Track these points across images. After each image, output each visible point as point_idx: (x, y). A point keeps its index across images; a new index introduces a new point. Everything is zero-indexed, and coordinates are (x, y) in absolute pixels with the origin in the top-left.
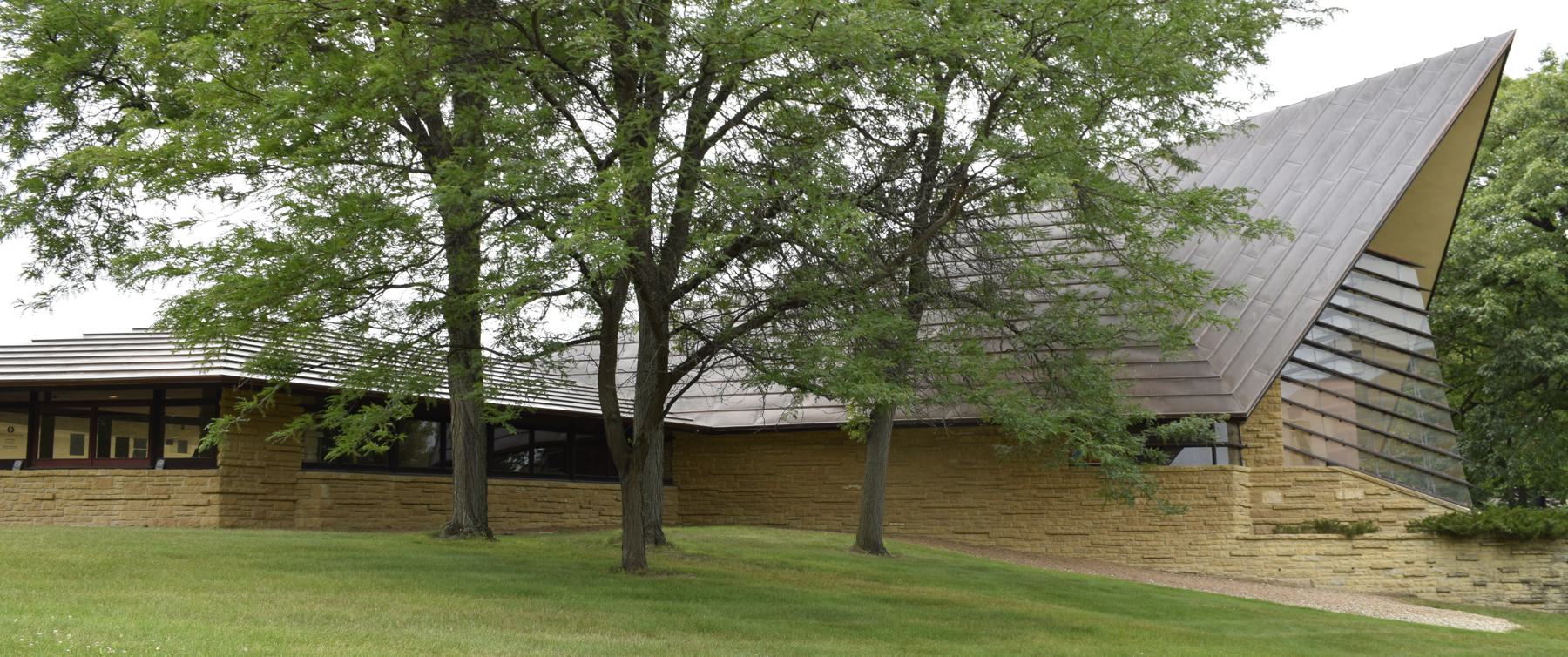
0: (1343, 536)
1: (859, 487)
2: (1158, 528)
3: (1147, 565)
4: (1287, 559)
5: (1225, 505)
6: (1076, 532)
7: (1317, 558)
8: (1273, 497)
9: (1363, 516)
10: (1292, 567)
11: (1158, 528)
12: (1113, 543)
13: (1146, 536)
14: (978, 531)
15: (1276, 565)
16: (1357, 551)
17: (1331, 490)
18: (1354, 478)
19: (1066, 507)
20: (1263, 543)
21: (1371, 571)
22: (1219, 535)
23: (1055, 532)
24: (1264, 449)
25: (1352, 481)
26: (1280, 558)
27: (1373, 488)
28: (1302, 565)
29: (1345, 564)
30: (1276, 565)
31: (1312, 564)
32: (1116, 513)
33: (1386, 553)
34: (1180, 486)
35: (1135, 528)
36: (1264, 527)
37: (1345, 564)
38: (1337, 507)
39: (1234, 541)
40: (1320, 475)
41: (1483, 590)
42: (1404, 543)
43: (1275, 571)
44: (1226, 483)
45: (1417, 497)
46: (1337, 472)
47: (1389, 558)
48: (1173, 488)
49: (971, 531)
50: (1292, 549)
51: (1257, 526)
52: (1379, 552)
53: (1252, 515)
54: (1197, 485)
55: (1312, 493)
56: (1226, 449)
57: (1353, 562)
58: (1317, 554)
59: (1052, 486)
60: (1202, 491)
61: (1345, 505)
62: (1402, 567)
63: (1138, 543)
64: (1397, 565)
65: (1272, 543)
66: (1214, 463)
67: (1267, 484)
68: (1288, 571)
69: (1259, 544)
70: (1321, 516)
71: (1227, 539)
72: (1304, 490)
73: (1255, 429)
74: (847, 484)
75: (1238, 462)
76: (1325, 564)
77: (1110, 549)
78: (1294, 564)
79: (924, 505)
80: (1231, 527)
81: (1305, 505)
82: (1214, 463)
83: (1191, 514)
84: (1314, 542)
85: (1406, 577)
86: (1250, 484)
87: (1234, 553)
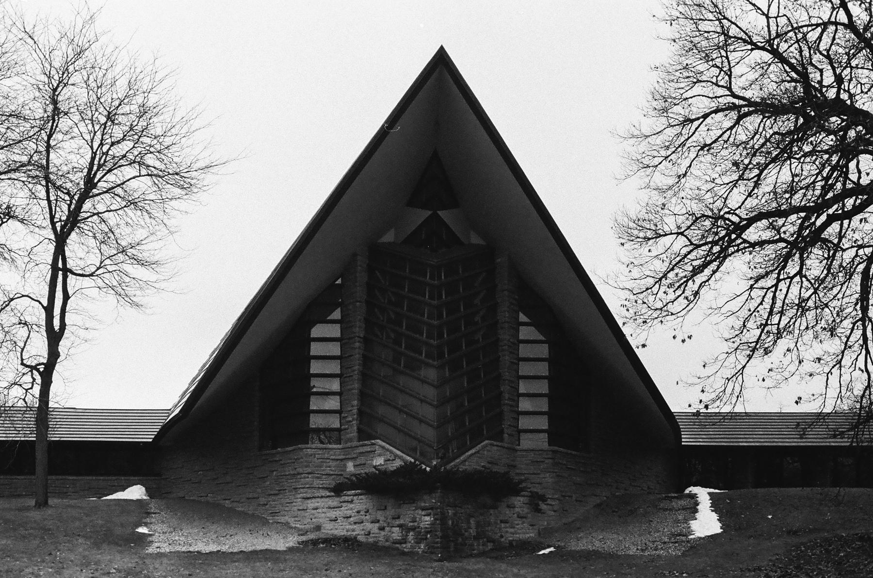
4: (315, 511)
11: (277, 492)
27: (388, 456)
29: (333, 514)
37: (333, 514)
46: (373, 444)
62: (355, 516)
69: (309, 501)
80: (302, 490)
83: (289, 481)
85: (355, 523)
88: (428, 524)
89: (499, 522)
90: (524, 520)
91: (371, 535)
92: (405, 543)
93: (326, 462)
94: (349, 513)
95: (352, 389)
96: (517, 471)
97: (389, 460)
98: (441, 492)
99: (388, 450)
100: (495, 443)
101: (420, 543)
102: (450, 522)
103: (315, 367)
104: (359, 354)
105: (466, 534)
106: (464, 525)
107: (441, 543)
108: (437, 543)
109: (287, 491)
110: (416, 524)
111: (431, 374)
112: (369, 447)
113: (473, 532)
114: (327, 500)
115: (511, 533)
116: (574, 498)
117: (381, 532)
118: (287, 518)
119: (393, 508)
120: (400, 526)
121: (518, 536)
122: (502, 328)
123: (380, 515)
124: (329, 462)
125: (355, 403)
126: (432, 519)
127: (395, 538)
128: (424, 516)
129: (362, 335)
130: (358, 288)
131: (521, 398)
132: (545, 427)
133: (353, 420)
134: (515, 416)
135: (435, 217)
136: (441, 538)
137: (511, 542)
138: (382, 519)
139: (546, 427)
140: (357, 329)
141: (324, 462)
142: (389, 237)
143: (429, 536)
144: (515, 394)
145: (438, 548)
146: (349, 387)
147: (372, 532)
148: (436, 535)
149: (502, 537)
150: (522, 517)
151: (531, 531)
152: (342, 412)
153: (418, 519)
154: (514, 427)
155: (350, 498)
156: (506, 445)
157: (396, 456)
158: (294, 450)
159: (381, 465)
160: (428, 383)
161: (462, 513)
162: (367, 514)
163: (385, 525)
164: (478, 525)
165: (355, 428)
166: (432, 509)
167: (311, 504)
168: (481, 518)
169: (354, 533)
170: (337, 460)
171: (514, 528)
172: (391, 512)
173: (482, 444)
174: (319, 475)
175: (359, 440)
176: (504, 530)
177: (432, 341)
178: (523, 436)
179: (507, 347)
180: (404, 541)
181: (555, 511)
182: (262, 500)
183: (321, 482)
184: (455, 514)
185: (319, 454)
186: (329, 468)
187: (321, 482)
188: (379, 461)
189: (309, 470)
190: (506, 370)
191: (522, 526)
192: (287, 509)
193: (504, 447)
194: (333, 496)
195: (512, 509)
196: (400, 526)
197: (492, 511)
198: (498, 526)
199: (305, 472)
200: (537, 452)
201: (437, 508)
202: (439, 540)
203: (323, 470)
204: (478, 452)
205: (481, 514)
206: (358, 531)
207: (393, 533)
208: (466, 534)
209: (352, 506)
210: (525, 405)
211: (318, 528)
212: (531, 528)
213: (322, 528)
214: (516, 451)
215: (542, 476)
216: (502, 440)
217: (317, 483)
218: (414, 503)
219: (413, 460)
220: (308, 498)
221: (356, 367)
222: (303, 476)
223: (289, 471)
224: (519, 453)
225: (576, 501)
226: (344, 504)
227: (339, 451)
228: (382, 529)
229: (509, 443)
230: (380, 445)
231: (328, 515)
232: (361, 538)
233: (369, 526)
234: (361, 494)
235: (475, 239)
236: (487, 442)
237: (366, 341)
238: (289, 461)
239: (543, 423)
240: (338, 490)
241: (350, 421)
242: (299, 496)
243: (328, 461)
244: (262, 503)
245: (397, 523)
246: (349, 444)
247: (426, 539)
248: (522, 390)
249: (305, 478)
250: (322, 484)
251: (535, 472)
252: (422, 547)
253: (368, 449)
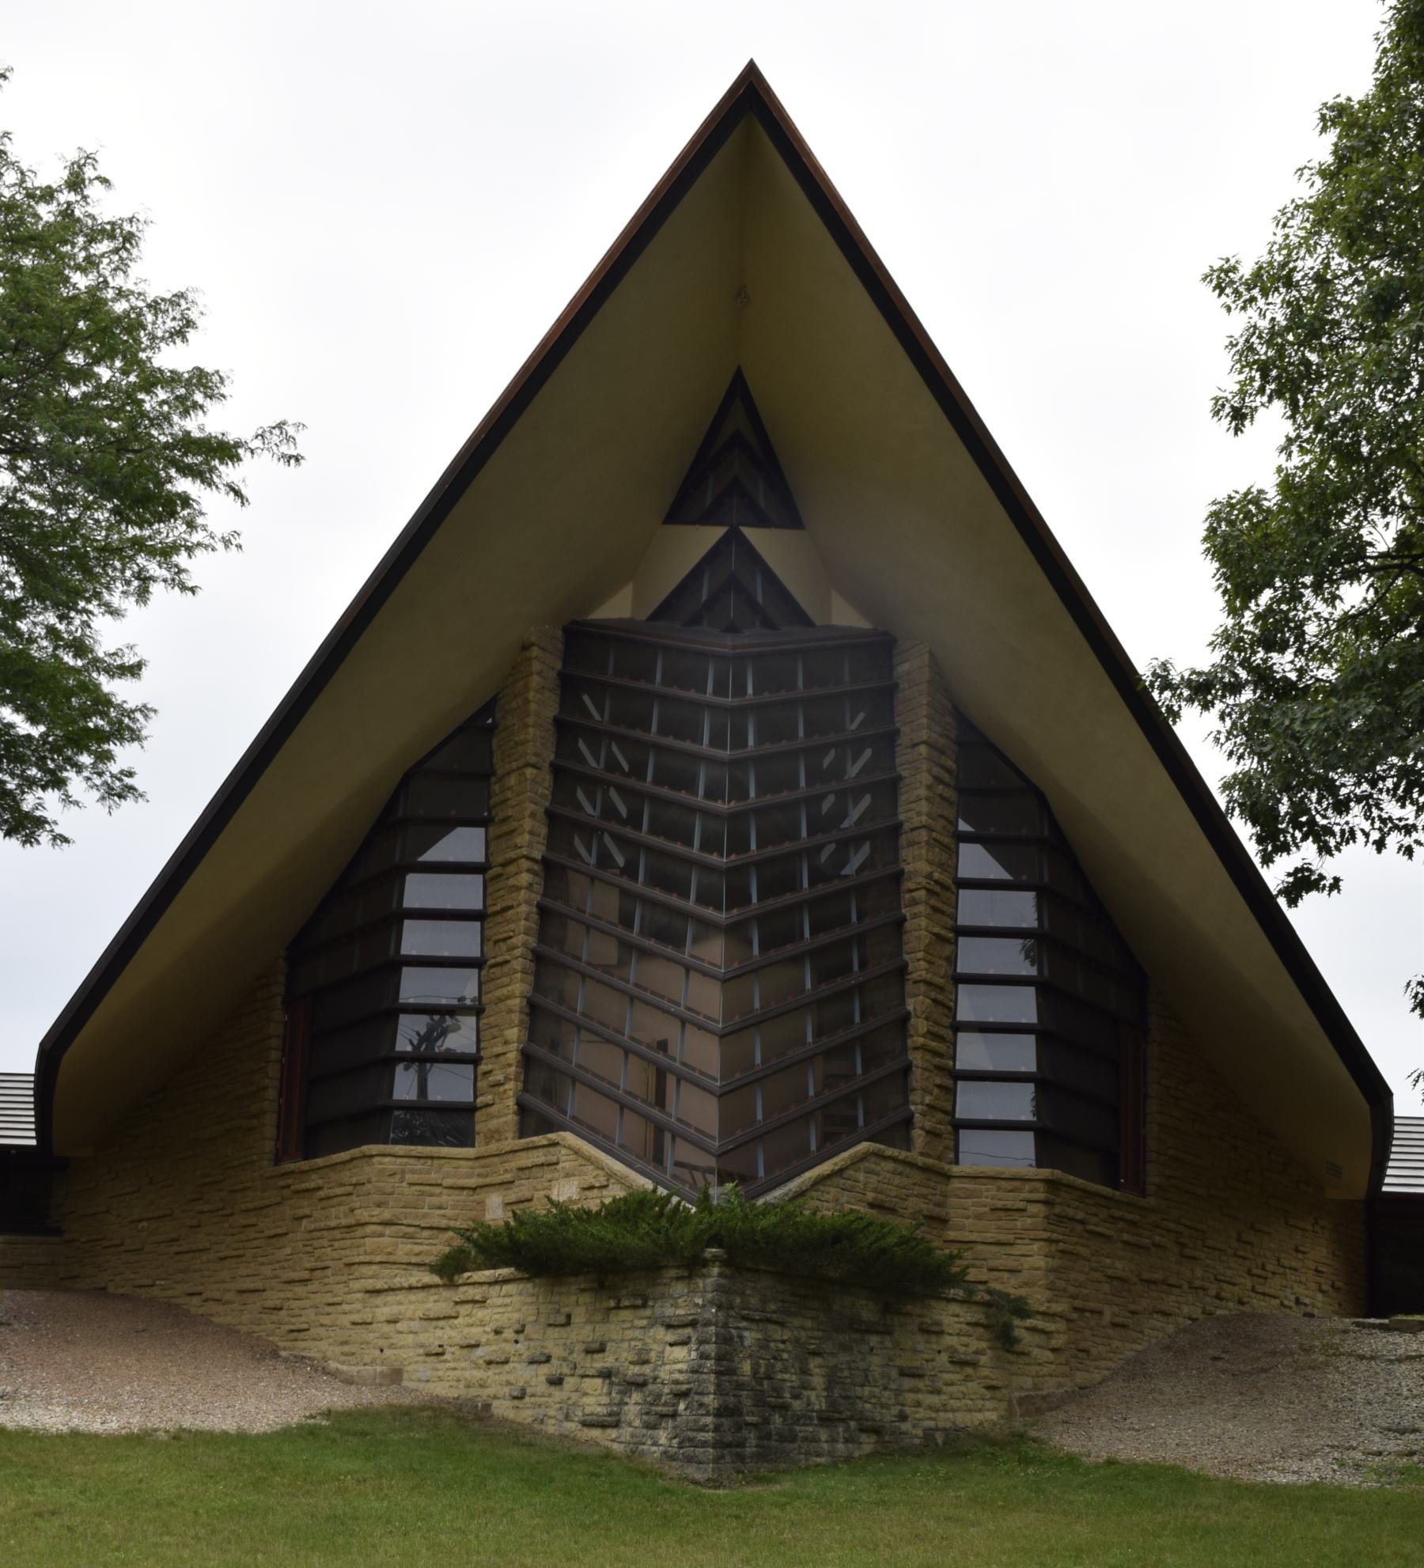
11: (306, 1275)
29: (434, 1336)
31: (410, 1338)
37: (434, 1336)
46: (555, 1144)
62: (488, 1343)
69: (379, 1300)
80: (365, 1270)
85: (489, 1363)
86: (473, 1182)
88: (680, 1372)
89: (894, 1373)
90: (969, 1370)
91: (527, 1399)
92: (616, 1425)
93: (432, 1195)
94: (475, 1334)
95: (508, 998)
96: (952, 1235)
97: (591, 1188)
98: (720, 1275)
99: (589, 1159)
100: (890, 1151)
101: (654, 1427)
102: (747, 1367)
103: (415, 939)
104: (527, 902)
105: (797, 1405)
106: (791, 1378)
107: (717, 1428)
108: (704, 1428)
109: (329, 1272)
110: (647, 1370)
111: (714, 951)
112: (541, 1152)
113: (817, 1399)
114: (421, 1295)
115: (930, 1408)
116: (1107, 1318)
117: (553, 1390)
118: (323, 1345)
119: (588, 1322)
120: (606, 1375)
121: (950, 1415)
122: (911, 844)
123: (553, 1342)
124: (440, 1195)
125: (513, 1033)
126: (694, 1355)
127: (588, 1410)
128: (671, 1345)
129: (538, 855)
130: (531, 730)
131: (961, 1036)
132: (1026, 1114)
133: (507, 1079)
134: (949, 1082)
135: (734, 538)
136: (719, 1413)
137: (929, 1434)
138: (556, 1351)
139: (1026, 1114)
140: (527, 837)
141: (422, 1194)
142: (618, 607)
143: (682, 1406)
144: (947, 1021)
145: (704, 1444)
146: (498, 993)
147: (529, 1390)
148: (701, 1405)
149: (903, 1417)
150: (963, 1363)
151: (988, 1404)
152: (482, 1058)
153: (653, 1355)
154: (945, 1112)
155: (475, 1293)
156: (921, 1160)
157: (611, 1175)
158: (352, 1160)
160: (705, 974)
161: (783, 1342)
162: (521, 1337)
163: (566, 1370)
164: (832, 1380)
165: (511, 1102)
166: (693, 1324)
167: (385, 1308)
168: (844, 1357)
169: (485, 1392)
170: (463, 1188)
171: (939, 1392)
172: (582, 1332)
173: (851, 1151)
174: (412, 1229)
175: (522, 1133)
176: (910, 1397)
177: (714, 859)
178: (969, 1140)
179: (923, 893)
180: (612, 1421)
181: (1054, 1350)
182: (272, 1298)
183: (418, 1248)
184: (763, 1345)
185: (413, 1172)
186: (438, 1212)
187: (418, 1248)
188: (566, 1191)
189: (387, 1215)
190: (920, 955)
191: (962, 1388)
192: (325, 1320)
193: (913, 1165)
194: (437, 1286)
195: (934, 1338)
196: (606, 1375)
197: (874, 1340)
198: (893, 1386)
199: (374, 1220)
200: (1003, 1183)
201: (707, 1324)
202: (709, 1420)
203: (425, 1216)
204: (839, 1173)
205: (845, 1348)
206: (495, 1387)
207: (586, 1394)
208: (797, 1405)
209: (481, 1313)
210: (972, 1052)
211: (396, 1375)
212: (988, 1394)
213: (405, 1376)
214: (948, 1177)
215: (1019, 1249)
216: (908, 1145)
217: (404, 1250)
218: (644, 1306)
219: (649, 1185)
220: (378, 1292)
221: (519, 940)
222: (369, 1229)
223: (338, 1216)
224: (955, 1184)
225: (1114, 1325)
226: (464, 1309)
227: (470, 1163)
228: (556, 1381)
229: (927, 1155)
230: (569, 1148)
231: (422, 1338)
232: (503, 1408)
233: (522, 1374)
234: (506, 1281)
235: (844, 616)
236: (864, 1146)
237: (550, 870)
238: (338, 1191)
239: (1019, 1103)
240: (450, 1268)
241: (499, 1084)
242: (355, 1285)
243: (438, 1190)
244: (270, 1304)
245: (598, 1365)
246: (493, 1147)
247: (674, 1415)
248: (965, 1012)
249: (374, 1235)
250: (417, 1254)
251: (1003, 1238)
252: (663, 1441)
253: (538, 1157)
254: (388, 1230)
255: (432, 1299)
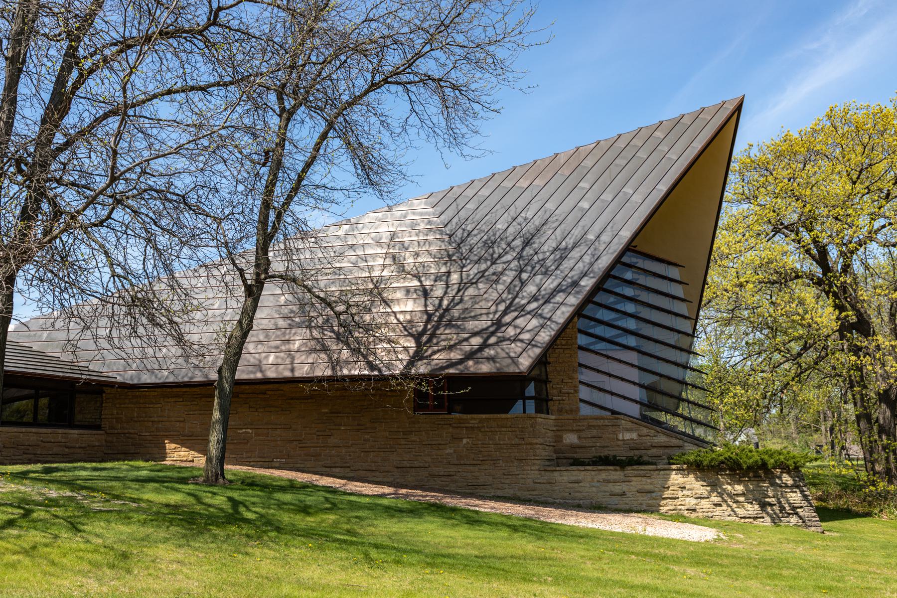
0: (618, 468)
1: (250, 431)
2: (479, 462)
3: (471, 491)
5: (531, 444)
6: (417, 465)
7: (598, 484)
8: (571, 438)
9: (637, 452)
10: (579, 492)
11: (479, 462)
12: (445, 474)
13: (472, 468)
14: (345, 465)
15: (567, 490)
16: (628, 479)
17: (614, 433)
18: (630, 424)
19: (411, 447)
20: (558, 473)
21: (638, 494)
22: (526, 468)
23: (401, 465)
24: (565, 402)
25: (629, 425)
26: (571, 485)
27: (645, 431)
28: (587, 489)
30: (567, 490)
31: (594, 489)
32: (448, 451)
33: (649, 481)
34: (497, 430)
35: (462, 462)
36: (565, 461)
37: (617, 488)
38: (618, 446)
39: (537, 472)
40: (606, 421)
41: (718, 508)
42: (662, 472)
43: (567, 494)
44: (532, 426)
45: (676, 438)
47: (651, 484)
48: (492, 432)
49: (337, 465)
50: (580, 478)
51: (559, 460)
52: (644, 479)
53: (555, 452)
54: (510, 429)
55: (600, 435)
56: (533, 401)
57: (624, 487)
58: (598, 481)
59: (400, 430)
60: (514, 433)
61: (624, 444)
63: (465, 474)
64: (656, 489)
65: (565, 473)
66: (524, 412)
67: (567, 428)
68: (577, 494)
69: (556, 474)
70: (605, 453)
71: (532, 470)
72: (594, 432)
73: (558, 386)
74: (241, 429)
75: (545, 411)
76: (604, 488)
77: (443, 478)
78: (580, 489)
79: (301, 445)
81: (594, 445)
82: (524, 412)
83: (505, 451)
84: (597, 472)
87: (536, 481)
94: (649, 487)
159: (632, 439)
254: (541, 447)
255: (604, 475)
